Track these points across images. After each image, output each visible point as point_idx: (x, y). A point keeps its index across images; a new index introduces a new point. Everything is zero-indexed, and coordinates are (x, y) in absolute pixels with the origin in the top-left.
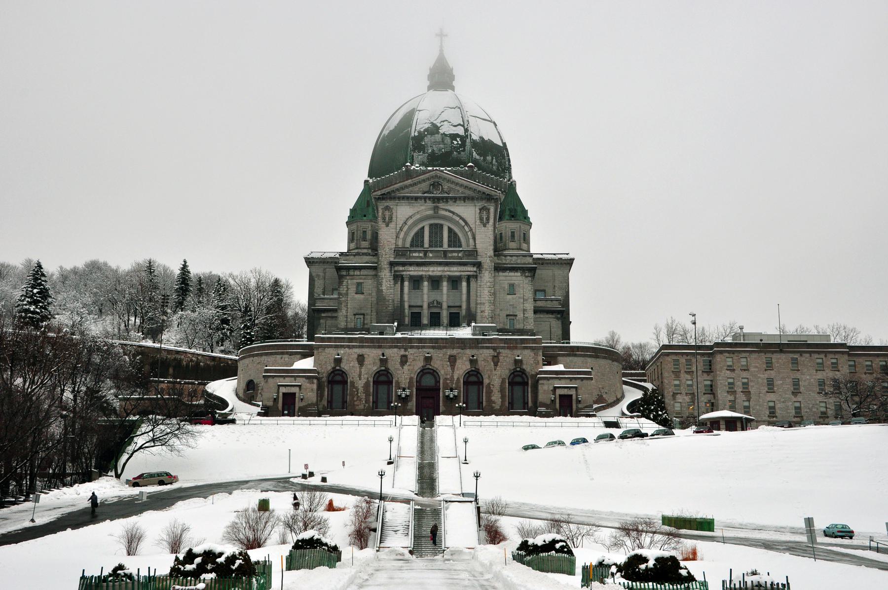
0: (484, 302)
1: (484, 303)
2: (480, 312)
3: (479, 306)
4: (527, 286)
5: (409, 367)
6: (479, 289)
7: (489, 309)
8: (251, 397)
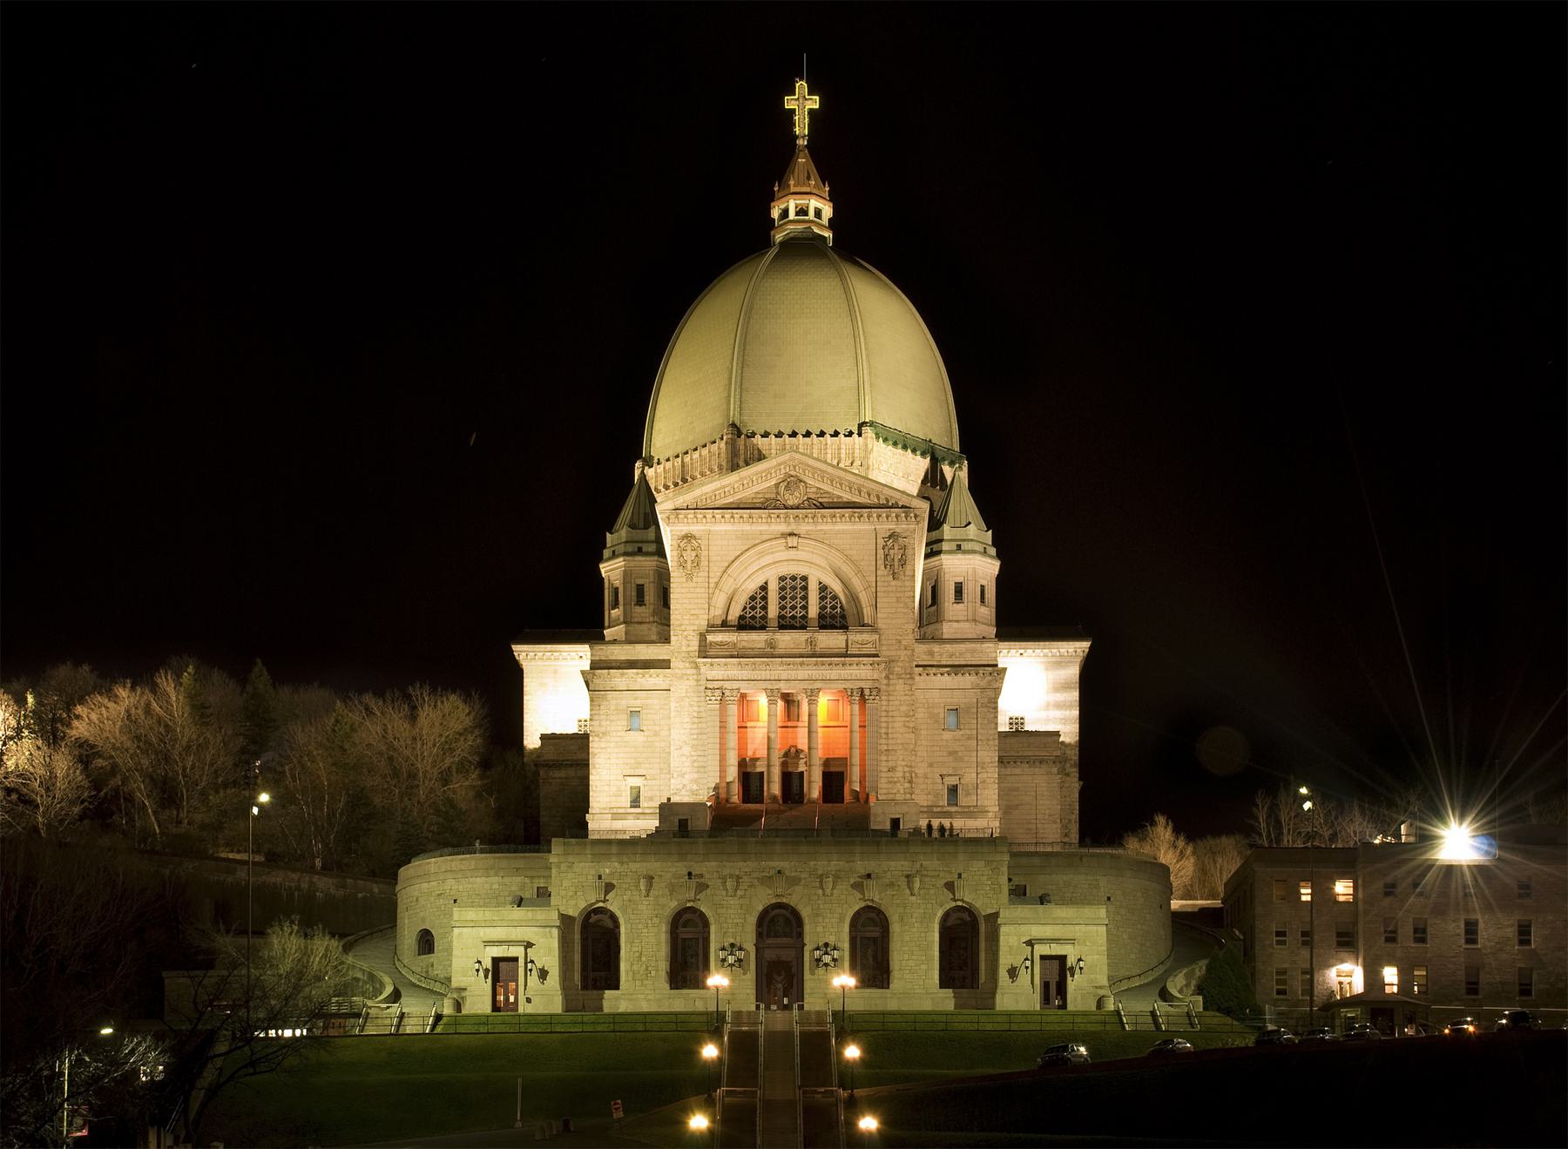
1: (895, 751)
3: (884, 758)
4: (986, 710)
5: (741, 901)
6: (884, 719)
7: (904, 763)
8: (427, 966)
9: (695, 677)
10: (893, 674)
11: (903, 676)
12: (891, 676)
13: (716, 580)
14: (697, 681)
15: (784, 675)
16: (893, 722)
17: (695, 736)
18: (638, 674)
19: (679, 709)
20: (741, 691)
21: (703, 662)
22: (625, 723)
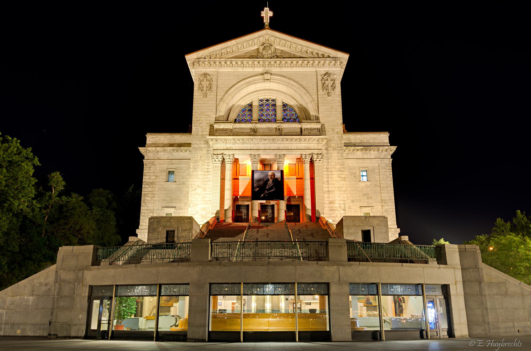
0: (333, 189)
1: (333, 191)
2: (328, 202)
4: (385, 171)
6: (325, 173)
7: (339, 199)
9: (206, 149)
10: (330, 148)
11: (337, 148)
12: (329, 149)
13: (221, 97)
14: (208, 151)
15: (262, 146)
16: (332, 174)
17: (205, 183)
18: (174, 150)
19: (196, 167)
20: (236, 157)
21: (211, 139)
22: (165, 177)
